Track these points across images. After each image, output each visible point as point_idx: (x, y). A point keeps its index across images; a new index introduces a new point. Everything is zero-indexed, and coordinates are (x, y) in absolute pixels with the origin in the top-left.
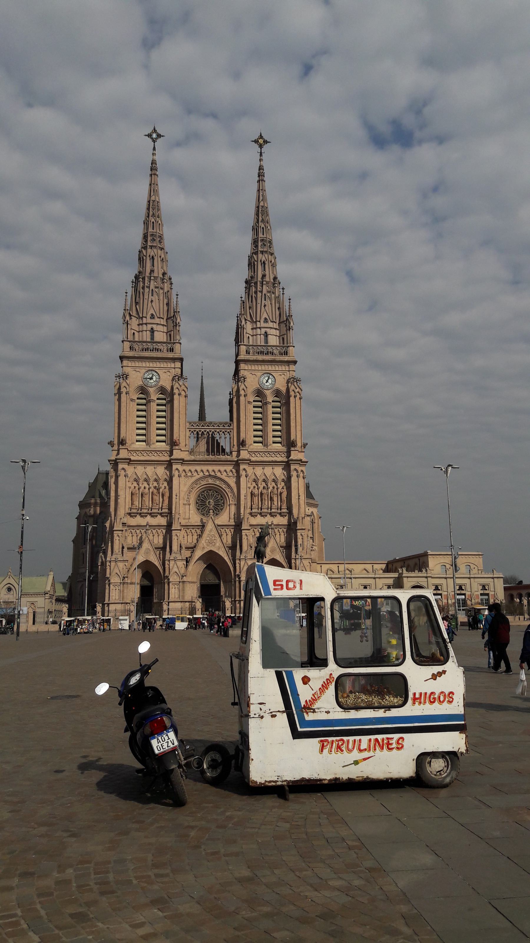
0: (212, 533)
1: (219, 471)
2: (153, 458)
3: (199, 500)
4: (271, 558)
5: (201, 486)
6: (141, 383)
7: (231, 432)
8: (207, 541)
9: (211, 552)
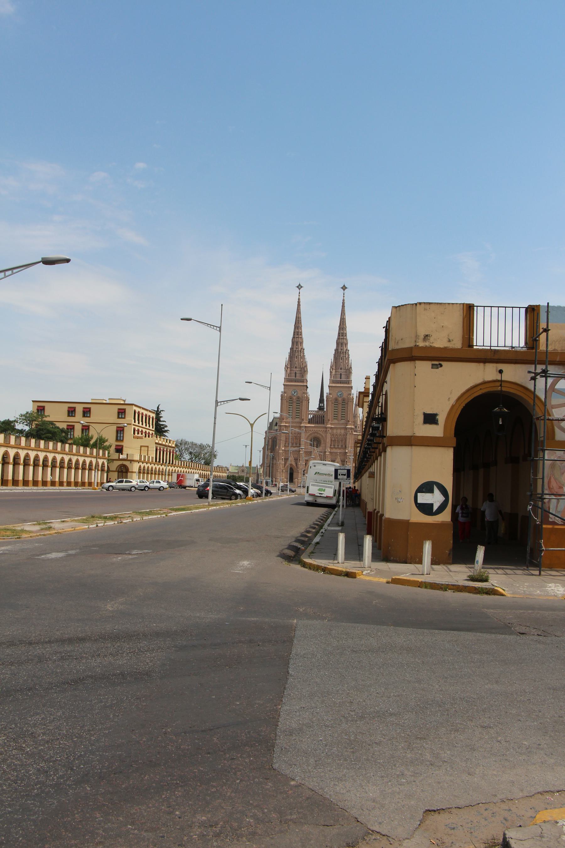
1: (319, 430)
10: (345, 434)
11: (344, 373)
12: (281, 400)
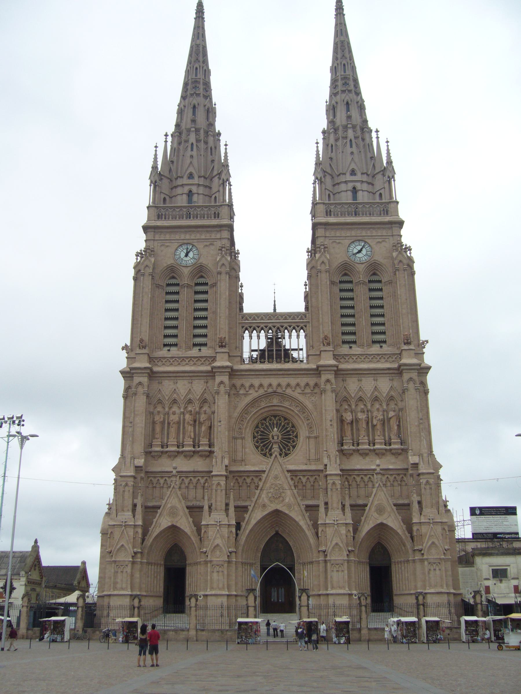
0: (278, 482)
1: (288, 385)
2: (187, 368)
3: (257, 433)
4: (379, 522)
5: (261, 409)
6: (170, 262)
7: (306, 326)
8: (270, 495)
9: (277, 513)
10: (392, 393)
11: (365, 186)
12: (135, 279)
